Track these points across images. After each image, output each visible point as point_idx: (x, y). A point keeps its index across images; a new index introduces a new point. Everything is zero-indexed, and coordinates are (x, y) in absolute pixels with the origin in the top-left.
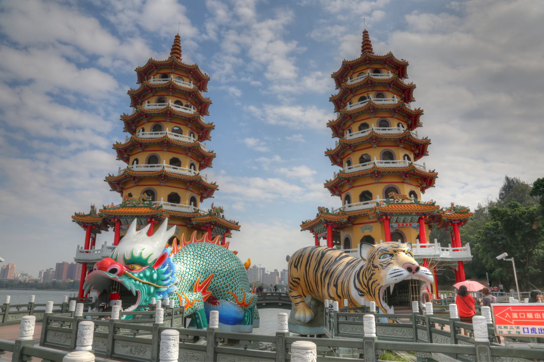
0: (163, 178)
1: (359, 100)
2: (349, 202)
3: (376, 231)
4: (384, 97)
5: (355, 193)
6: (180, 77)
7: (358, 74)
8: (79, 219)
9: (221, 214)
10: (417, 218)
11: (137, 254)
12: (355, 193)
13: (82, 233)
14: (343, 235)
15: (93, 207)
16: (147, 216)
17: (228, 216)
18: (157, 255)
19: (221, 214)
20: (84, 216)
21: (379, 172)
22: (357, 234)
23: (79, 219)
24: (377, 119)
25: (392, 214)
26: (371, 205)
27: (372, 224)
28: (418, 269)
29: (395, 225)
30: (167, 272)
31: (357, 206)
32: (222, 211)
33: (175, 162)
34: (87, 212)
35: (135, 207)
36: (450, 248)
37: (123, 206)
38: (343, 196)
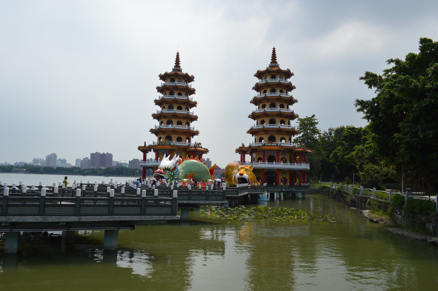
0: (175, 131)
6: (180, 81)
8: (140, 148)
9: (200, 146)
11: (167, 167)
13: (142, 154)
15: (145, 143)
16: (169, 150)
17: (204, 146)
18: (173, 167)
19: (200, 146)
20: (142, 147)
23: (140, 148)
24: (270, 103)
28: (243, 175)
30: (176, 172)
32: (200, 144)
33: (179, 123)
34: (143, 145)
35: (163, 145)
36: (295, 164)
37: (159, 144)
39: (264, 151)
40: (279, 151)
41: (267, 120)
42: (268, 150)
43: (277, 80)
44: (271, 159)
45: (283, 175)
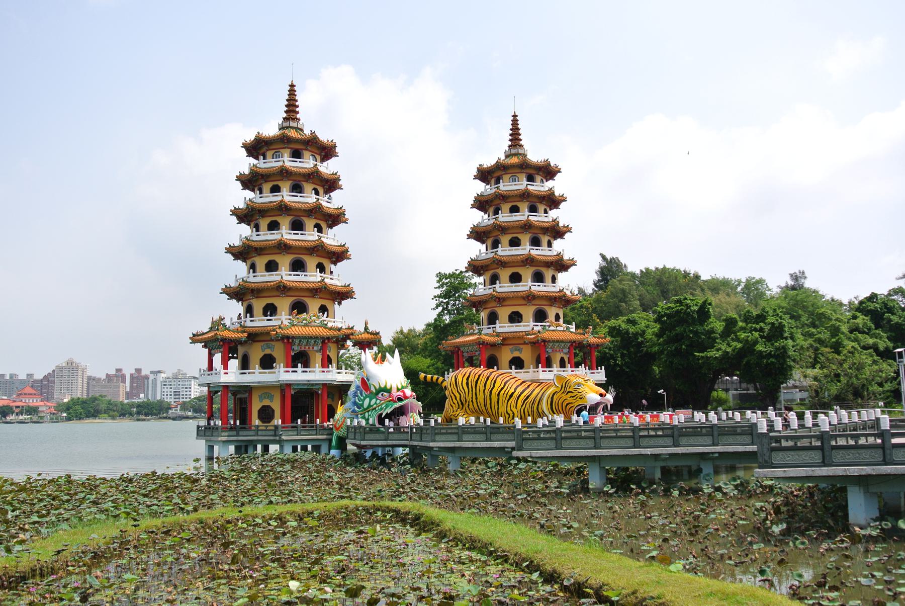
1: (271, 192)
2: (252, 316)
3: (278, 351)
4: (300, 192)
5: (259, 305)
7: (273, 151)
10: (320, 342)
12: (259, 305)
14: (241, 350)
21: (285, 287)
22: (257, 353)
25: (293, 337)
26: (274, 322)
27: (273, 343)
29: (297, 348)
31: (259, 322)
38: (246, 304)
39: (287, 340)
40: (328, 338)
41: (284, 261)
42: (301, 338)
43: (308, 163)
44: (300, 359)
45: (261, 402)
